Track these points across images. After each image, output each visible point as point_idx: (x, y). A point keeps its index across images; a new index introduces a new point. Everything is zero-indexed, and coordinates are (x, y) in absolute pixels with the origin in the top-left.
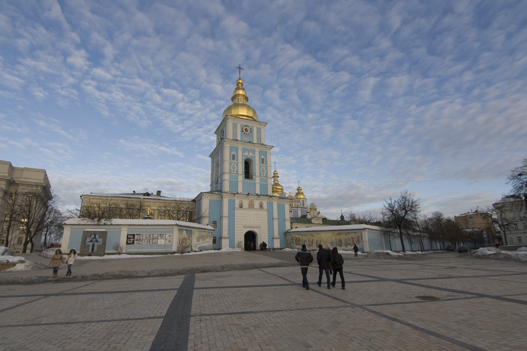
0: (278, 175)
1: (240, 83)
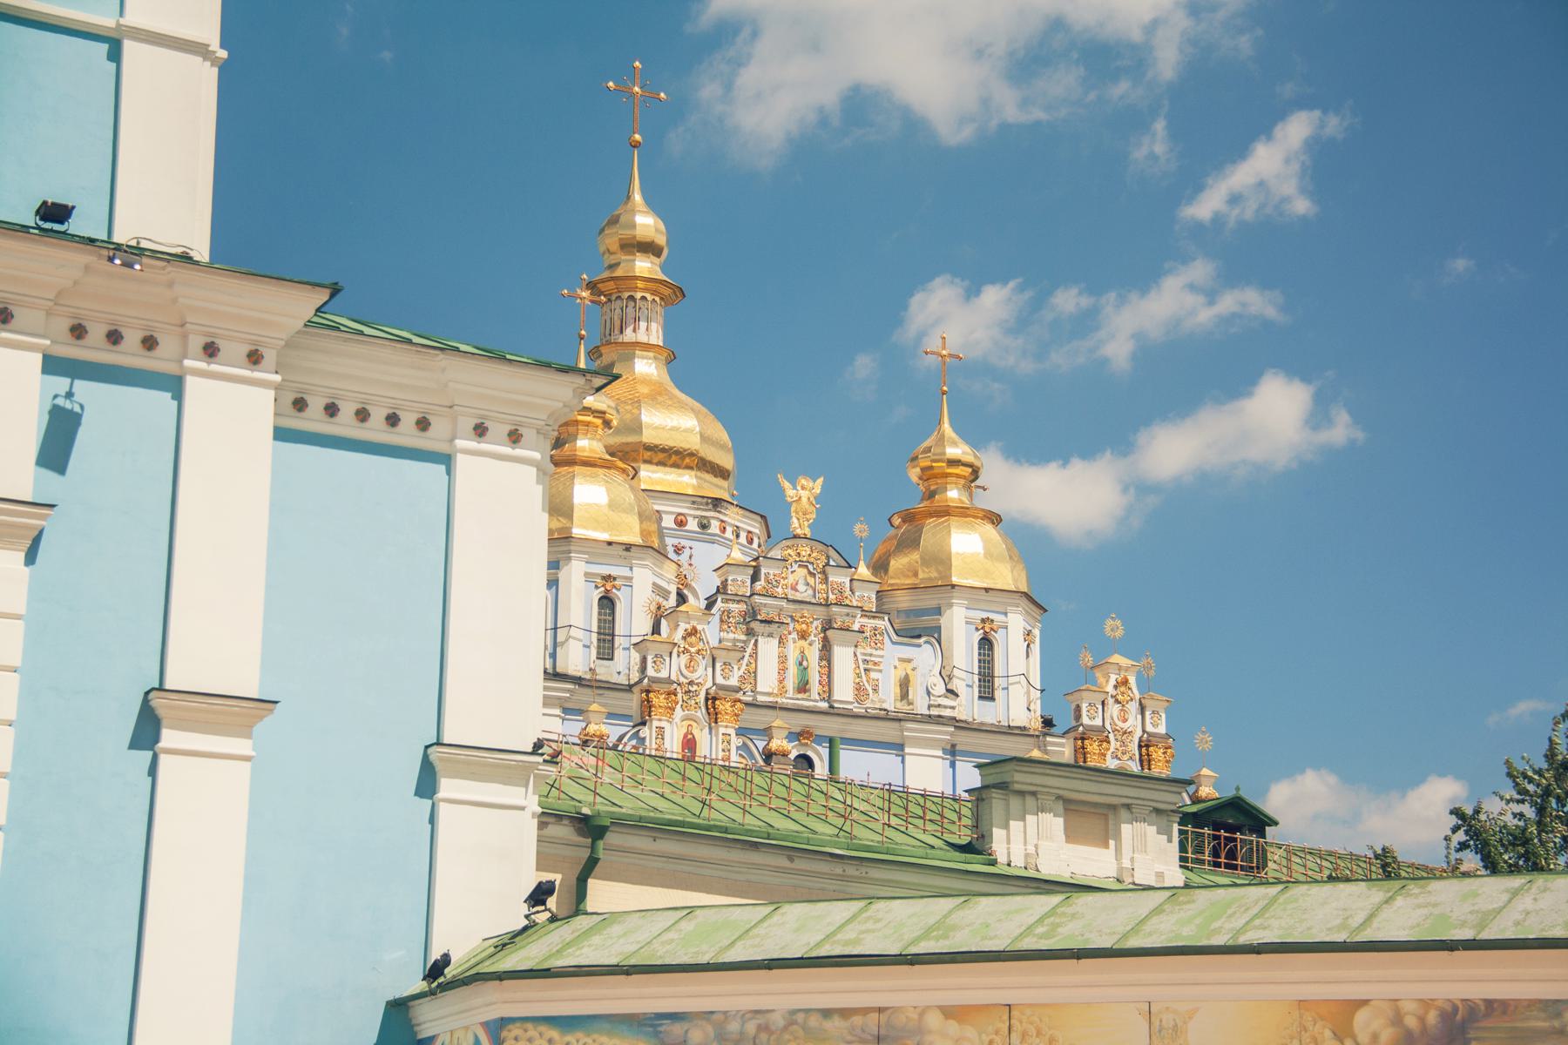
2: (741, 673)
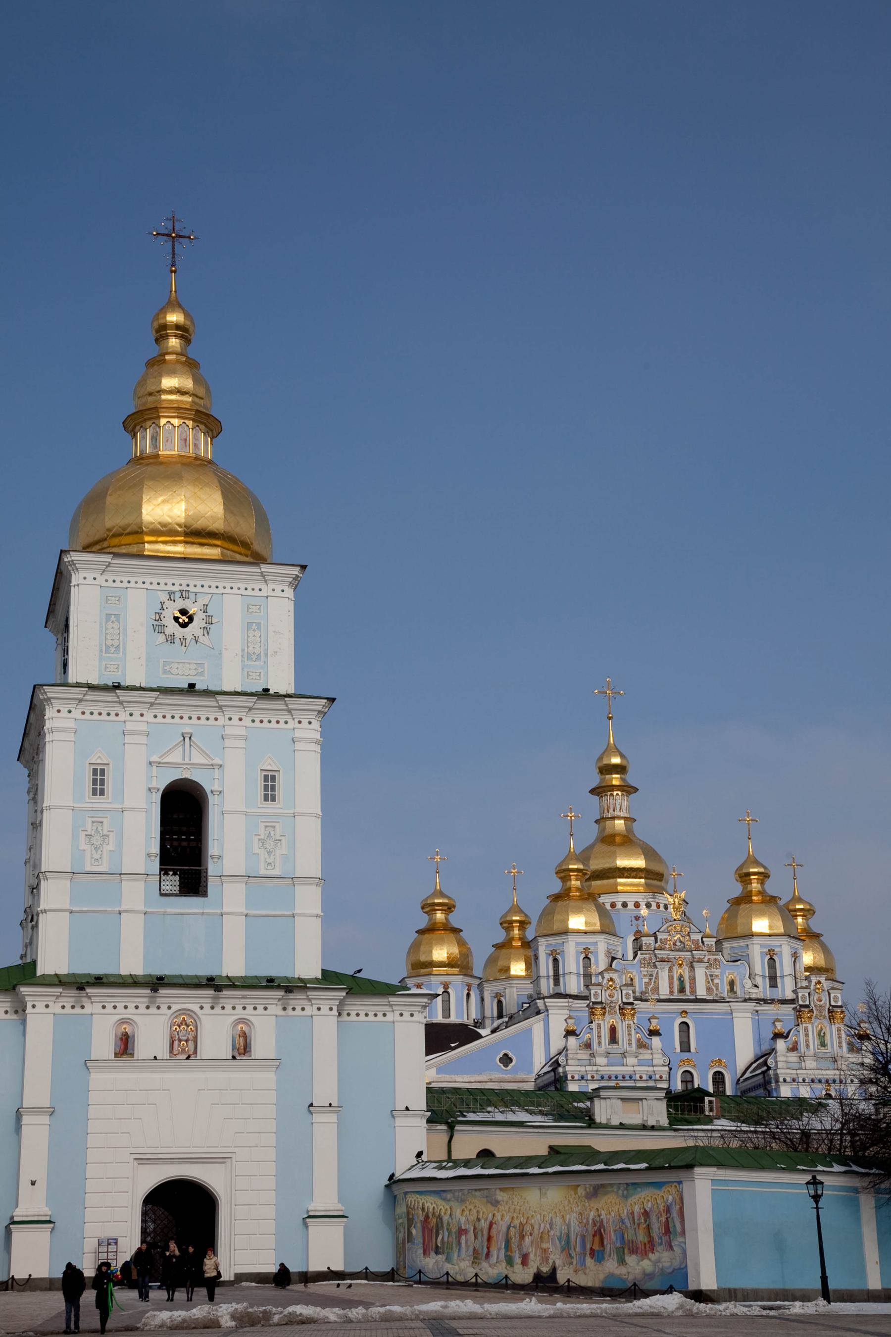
0: (632, 779)
1: (178, 327)
2: (651, 986)
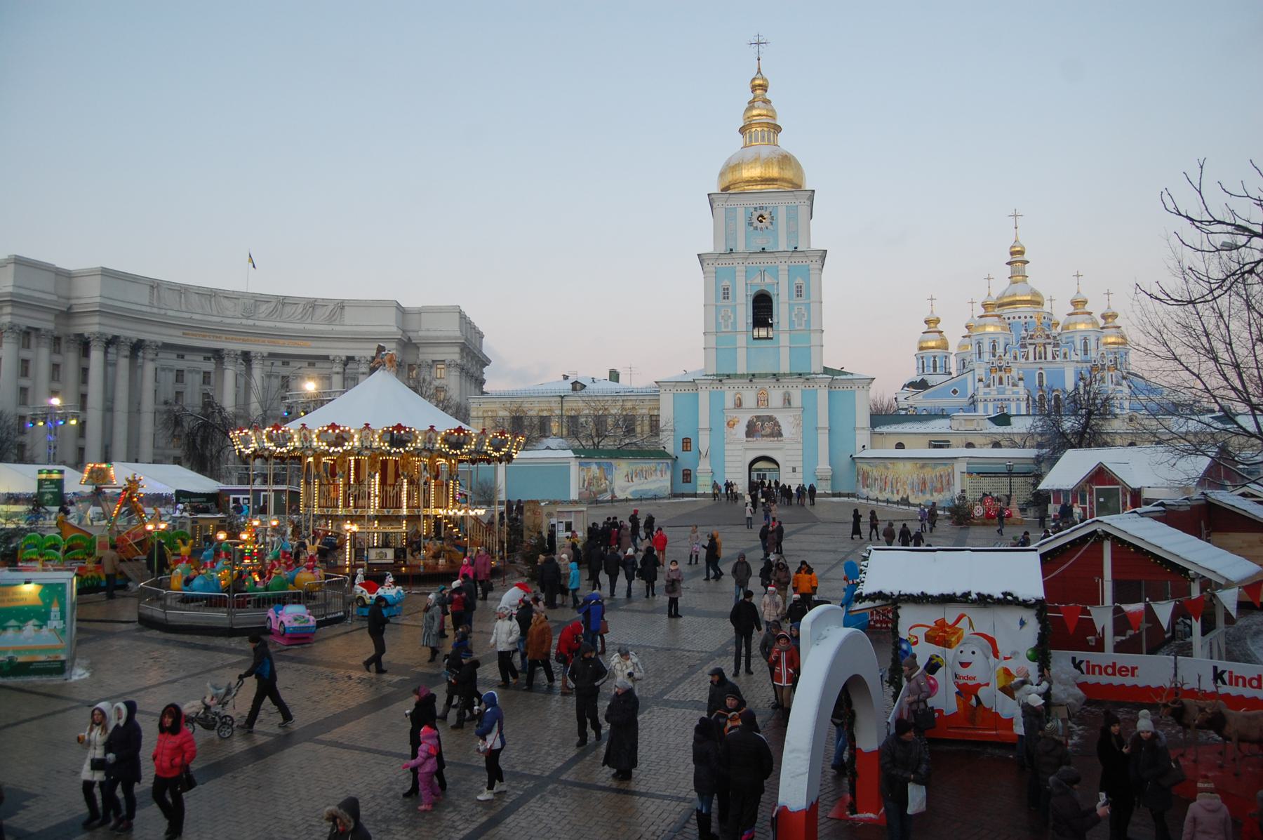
0: (1026, 257)
1: (760, 85)
